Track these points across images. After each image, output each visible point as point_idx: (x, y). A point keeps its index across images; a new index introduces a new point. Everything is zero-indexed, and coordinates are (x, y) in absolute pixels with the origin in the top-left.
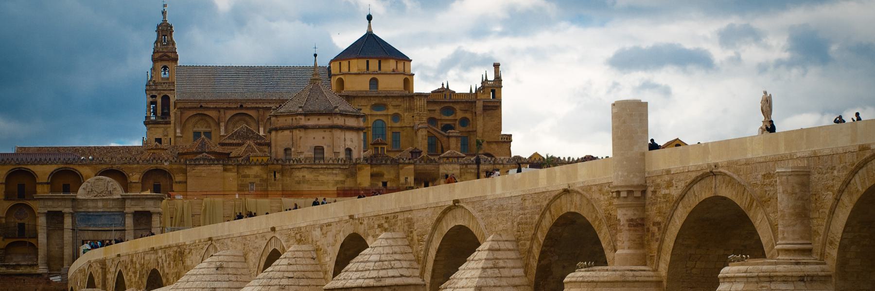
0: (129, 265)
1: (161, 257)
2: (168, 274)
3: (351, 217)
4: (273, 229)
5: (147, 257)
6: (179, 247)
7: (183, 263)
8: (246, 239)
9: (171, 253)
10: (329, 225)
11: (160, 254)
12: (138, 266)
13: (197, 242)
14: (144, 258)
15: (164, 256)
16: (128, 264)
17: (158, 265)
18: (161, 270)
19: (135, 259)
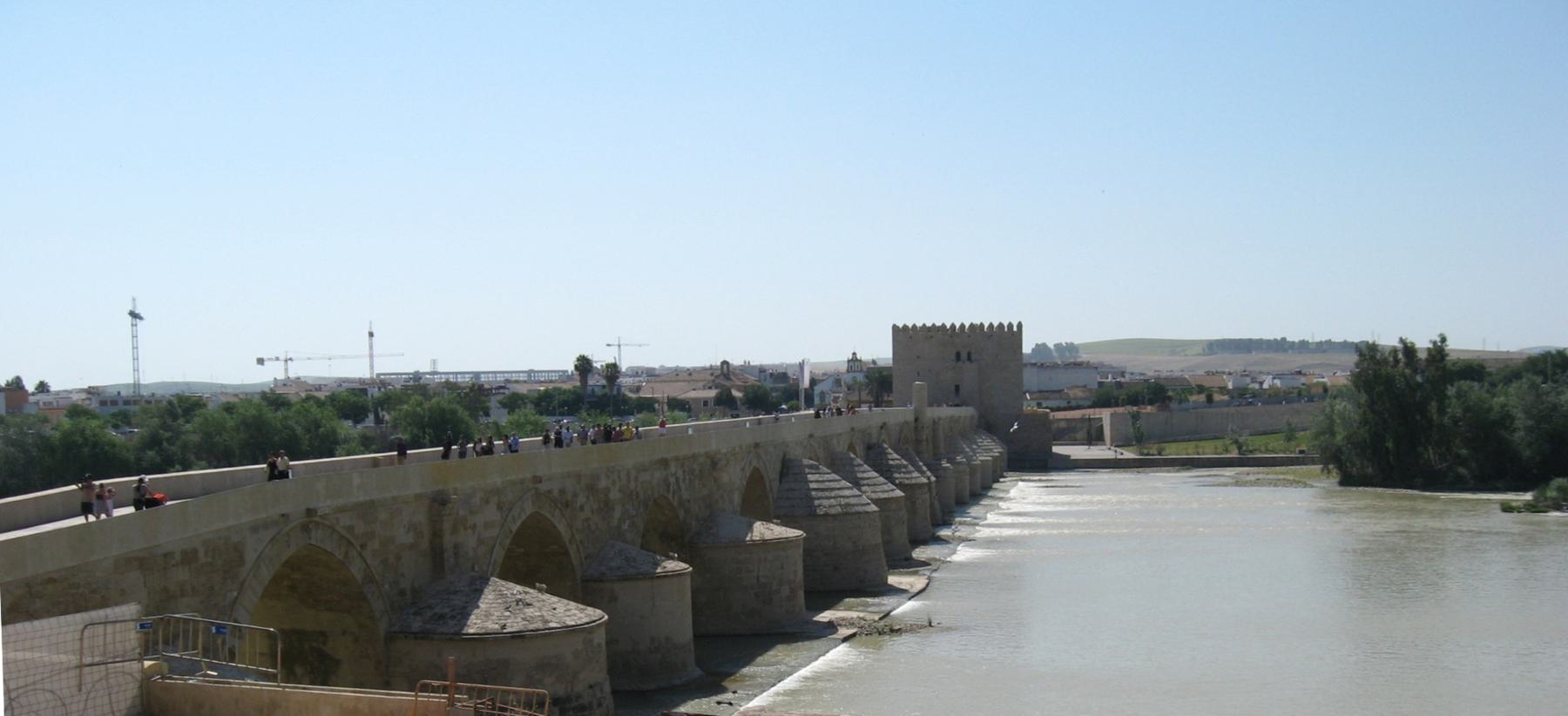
0: (581, 499)
1: (675, 474)
2: (689, 501)
3: (853, 429)
4: (811, 436)
5: (645, 477)
6: (707, 455)
7: (715, 481)
8: (787, 446)
9: (695, 466)
10: (840, 435)
11: (673, 469)
12: (615, 495)
13: (737, 449)
14: (636, 478)
15: (680, 473)
16: (575, 495)
17: (668, 491)
18: (674, 498)
19: (603, 483)
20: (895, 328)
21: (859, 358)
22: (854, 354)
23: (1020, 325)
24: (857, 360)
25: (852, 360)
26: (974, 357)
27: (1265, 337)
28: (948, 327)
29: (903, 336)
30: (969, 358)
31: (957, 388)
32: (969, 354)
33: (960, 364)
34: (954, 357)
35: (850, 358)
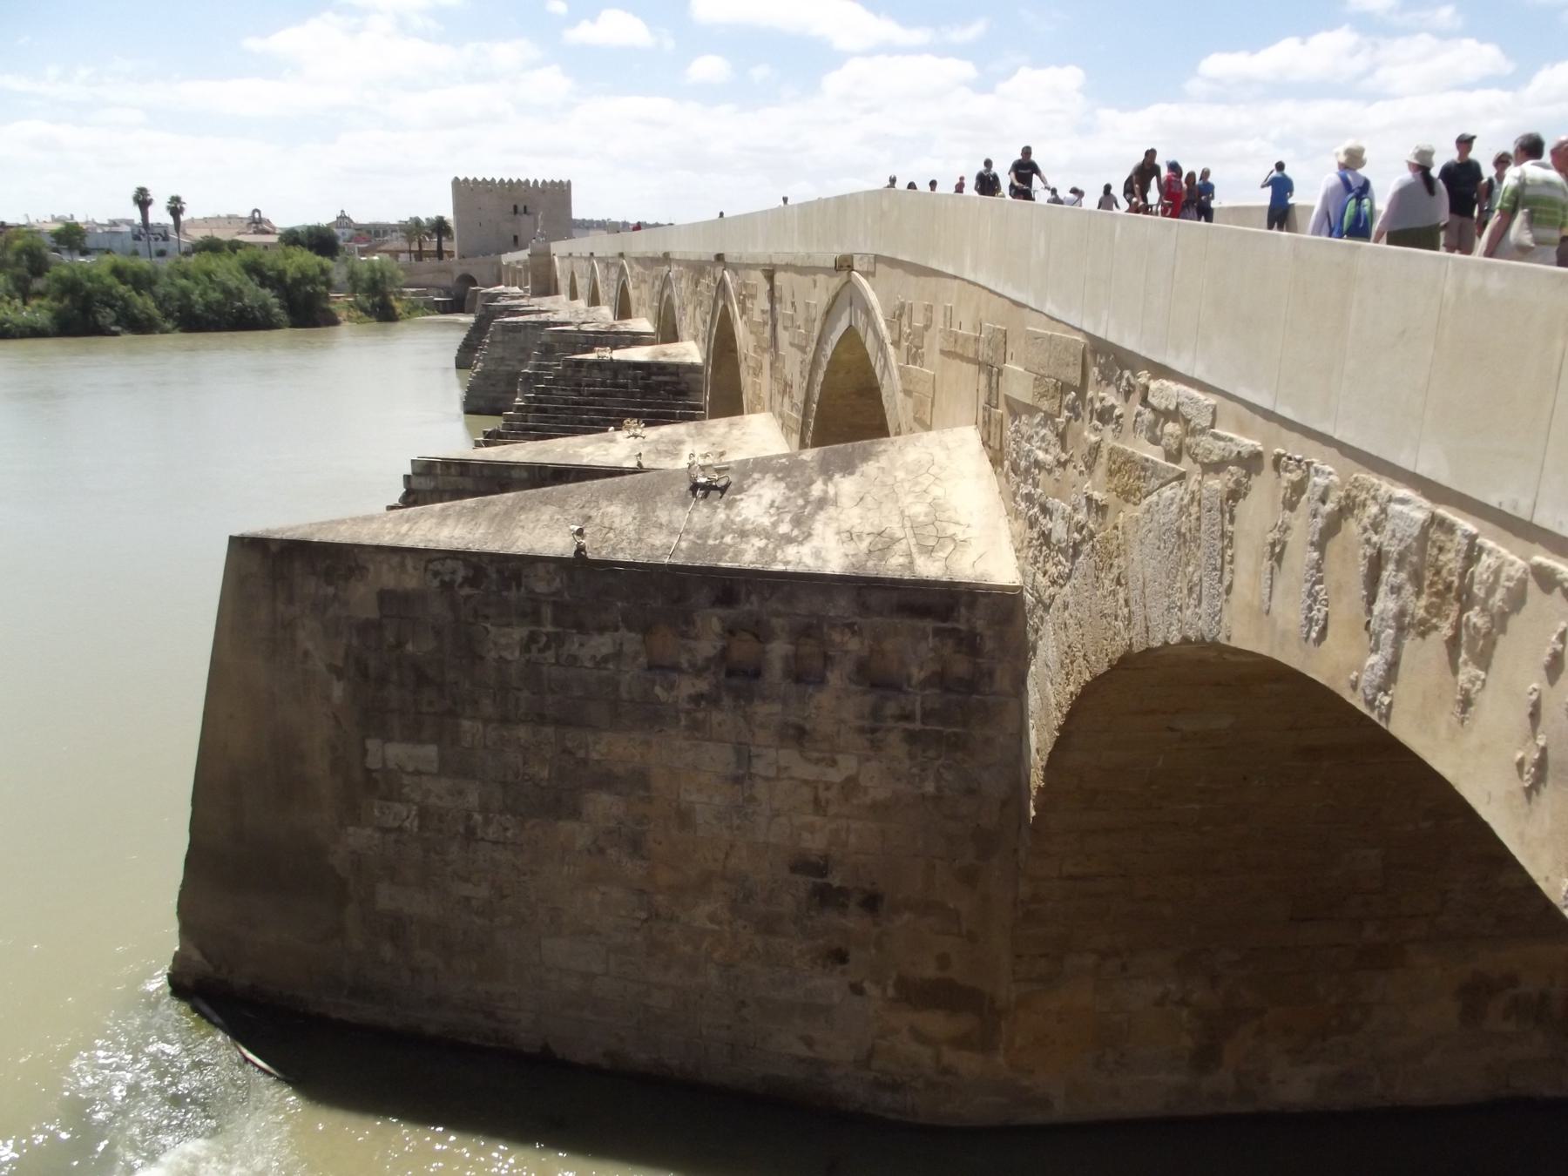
20: (457, 179)
21: (347, 215)
22: (342, 211)
23: (569, 183)
24: (345, 217)
25: (341, 217)
26: (529, 210)
27: (595, 219)
28: (497, 182)
29: (465, 190)
30: (525, 212)
31: (516, 238)
32: (525, 207)
33: (518, 216)
34: (512, 209)
35: (339, 214)
